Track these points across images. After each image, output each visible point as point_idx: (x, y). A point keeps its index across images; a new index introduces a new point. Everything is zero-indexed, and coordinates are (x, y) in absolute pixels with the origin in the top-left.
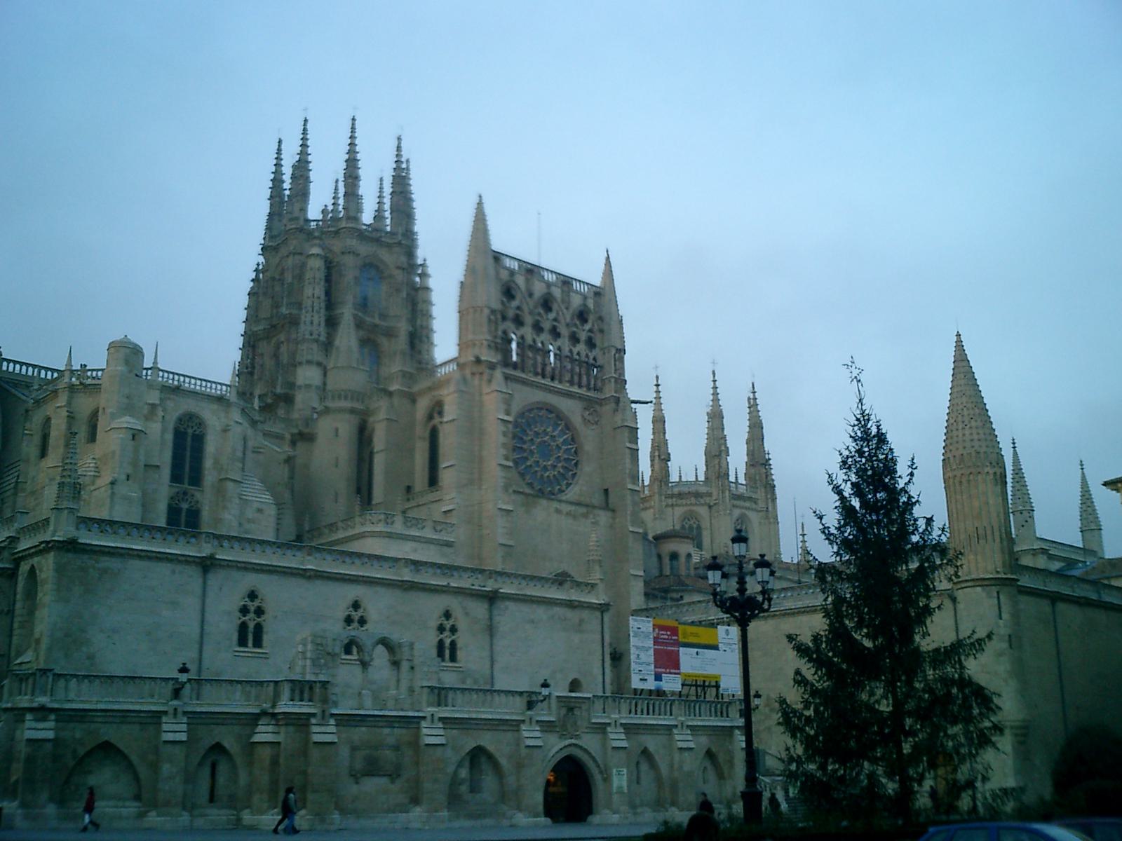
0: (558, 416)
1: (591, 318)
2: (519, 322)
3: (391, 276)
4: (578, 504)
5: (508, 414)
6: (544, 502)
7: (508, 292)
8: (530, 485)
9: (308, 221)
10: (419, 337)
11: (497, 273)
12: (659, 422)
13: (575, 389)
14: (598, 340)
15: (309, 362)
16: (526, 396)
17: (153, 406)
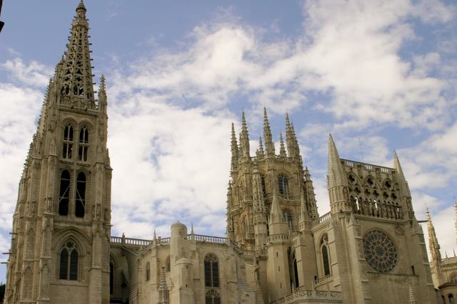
0: (384, 235)
1: (392, 185)
2: (358, 191)
3: (292, 178)
4: (399, 275)
5: (359, 235)
6: (383, 276)
7: (351, 178)
8: (375, 268)
9: (251, 158)
10: (310, 205)
11: (344, 169)
12: (432, 230)
13: (390, 219)
14: (397, 194)
15: (260, 223)
16: (369, 225)
17: (194, 252)
